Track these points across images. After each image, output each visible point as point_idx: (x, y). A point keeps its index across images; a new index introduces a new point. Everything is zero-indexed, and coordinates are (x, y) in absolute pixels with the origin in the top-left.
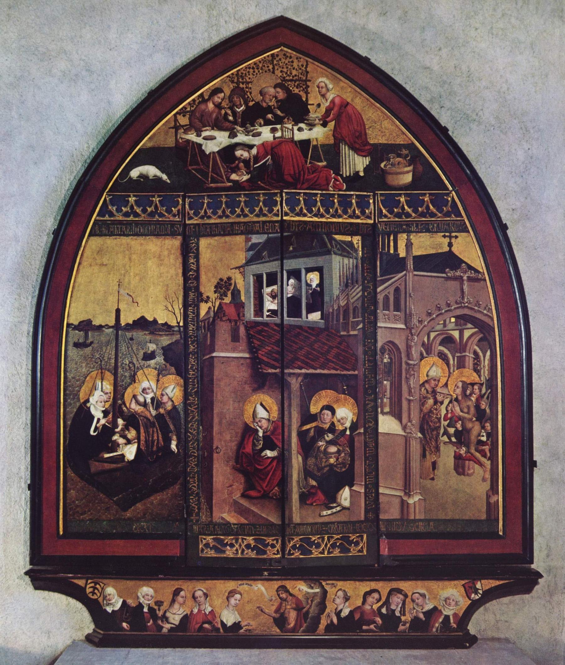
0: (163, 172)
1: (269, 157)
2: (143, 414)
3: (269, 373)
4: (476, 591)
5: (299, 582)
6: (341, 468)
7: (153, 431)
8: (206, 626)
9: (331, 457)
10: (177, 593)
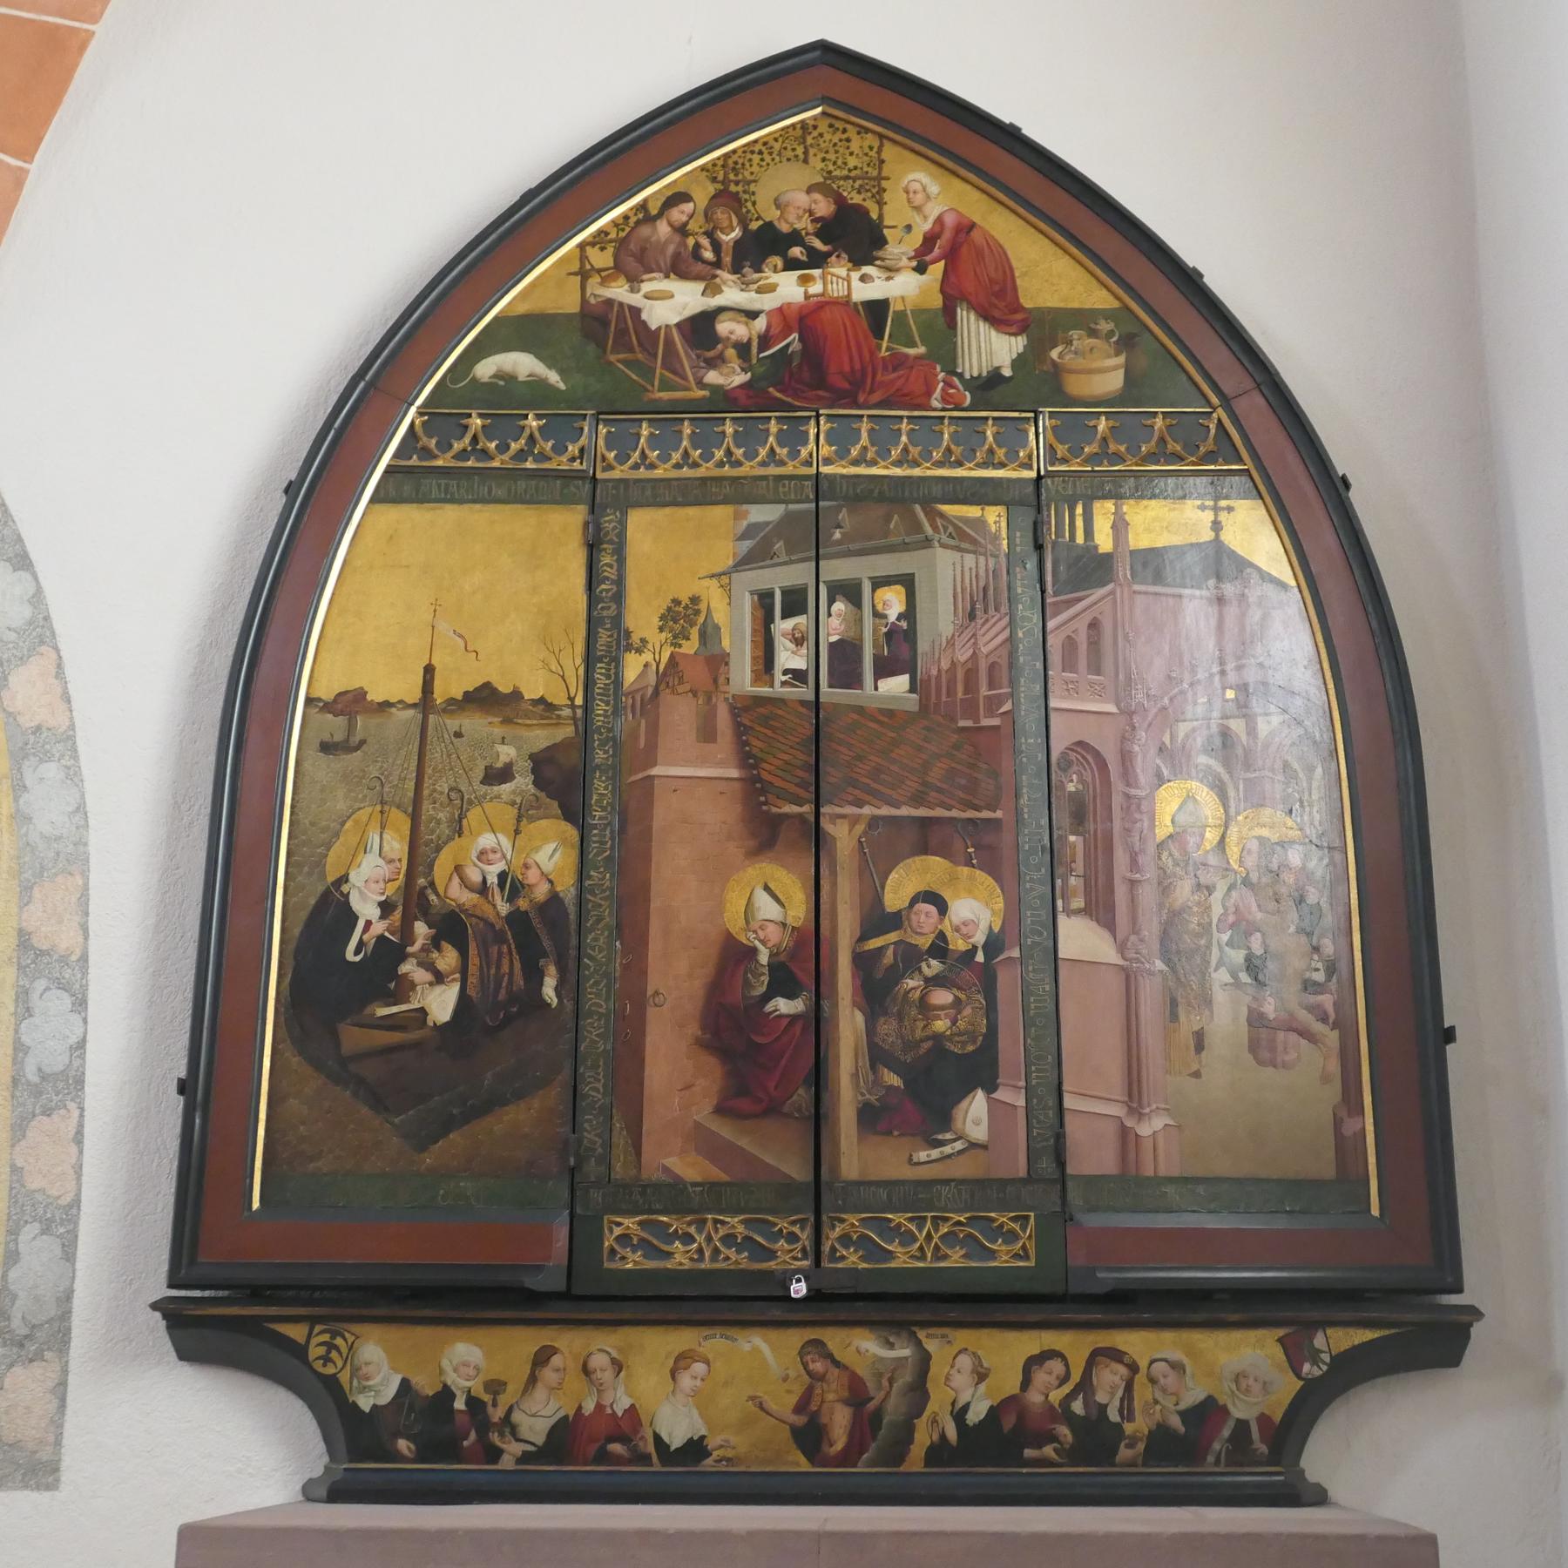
0: (550, 367)
1: (795, 335)
2: (478, 913)
3: (787, 816)
4: (1315, 1358)
5: (858, 1331)
6: (964, 1044)
7: (500, 954)
8: (616, 1448)
9: (938, 1018)
10: (543, 1357)
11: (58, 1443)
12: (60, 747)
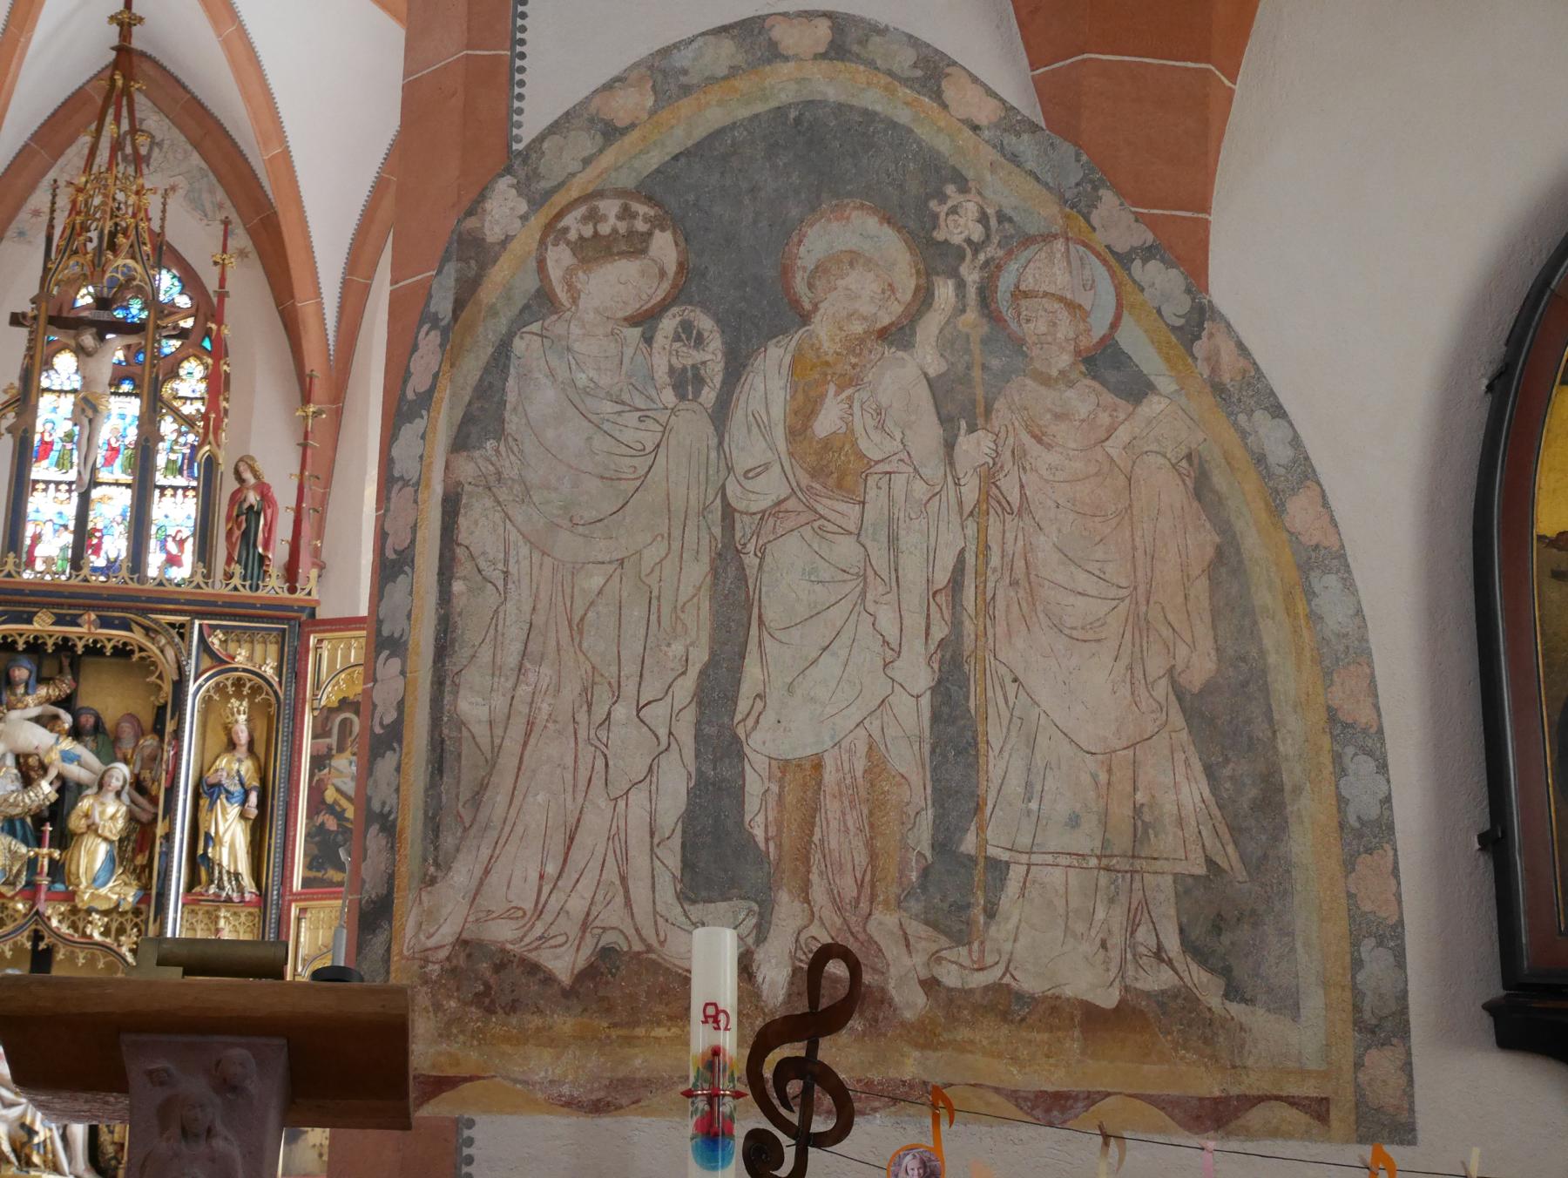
11: (1412, 1110)
12: (1335, 562)
